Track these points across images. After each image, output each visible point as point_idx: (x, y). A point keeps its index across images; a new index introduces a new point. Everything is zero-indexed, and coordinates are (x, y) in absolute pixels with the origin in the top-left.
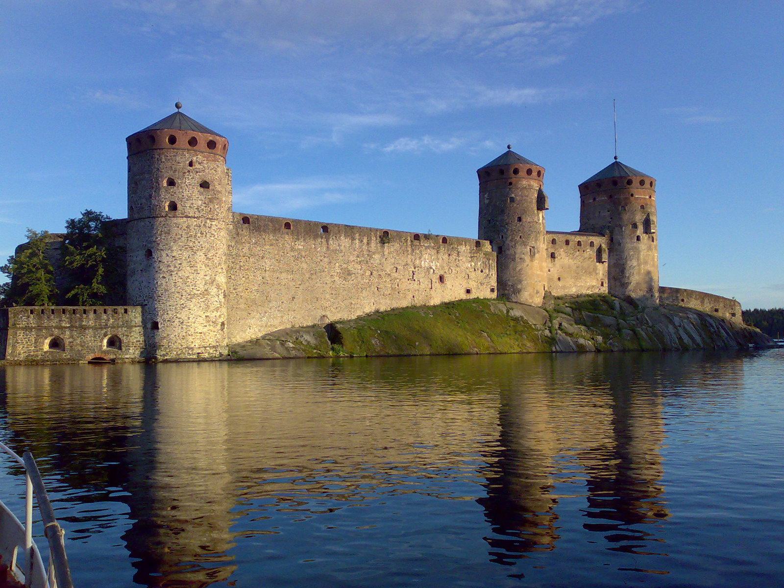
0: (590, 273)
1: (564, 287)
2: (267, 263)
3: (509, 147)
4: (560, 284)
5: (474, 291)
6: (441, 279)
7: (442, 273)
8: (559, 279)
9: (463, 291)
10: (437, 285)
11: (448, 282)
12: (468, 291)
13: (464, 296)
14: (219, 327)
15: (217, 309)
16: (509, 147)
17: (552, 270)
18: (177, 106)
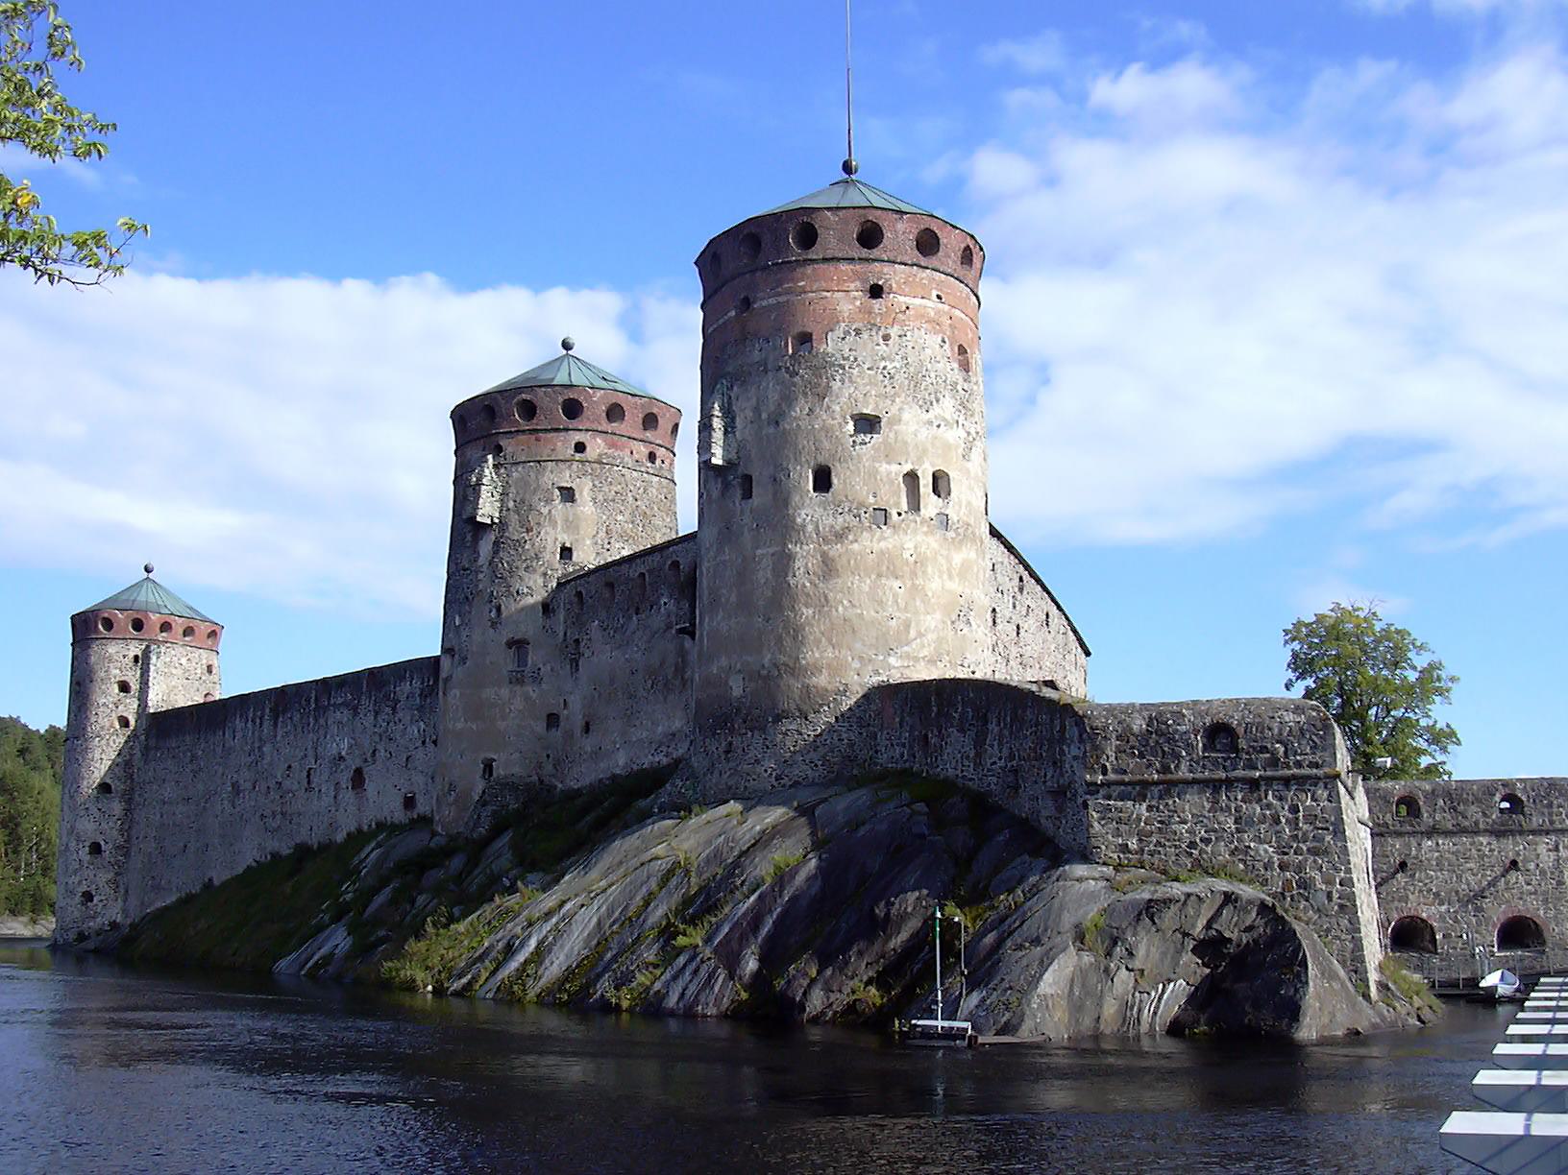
0: (667, 686)
1: (597, 754)
2: (168, 791)
3: (567, 346)
4: (588, 744)
5: (420, 799)
6: (358, 779)
7: (358, 763)
8: (587, 729)
9: (398, 803)
10: (348, 796)
11: (370, 787)
12: (409, 802)
13: (400, 816)
14: (78, 899)
15: (75, 872)
16: (567, 346)
17: (571, 699)
18: (148, 570)
